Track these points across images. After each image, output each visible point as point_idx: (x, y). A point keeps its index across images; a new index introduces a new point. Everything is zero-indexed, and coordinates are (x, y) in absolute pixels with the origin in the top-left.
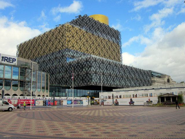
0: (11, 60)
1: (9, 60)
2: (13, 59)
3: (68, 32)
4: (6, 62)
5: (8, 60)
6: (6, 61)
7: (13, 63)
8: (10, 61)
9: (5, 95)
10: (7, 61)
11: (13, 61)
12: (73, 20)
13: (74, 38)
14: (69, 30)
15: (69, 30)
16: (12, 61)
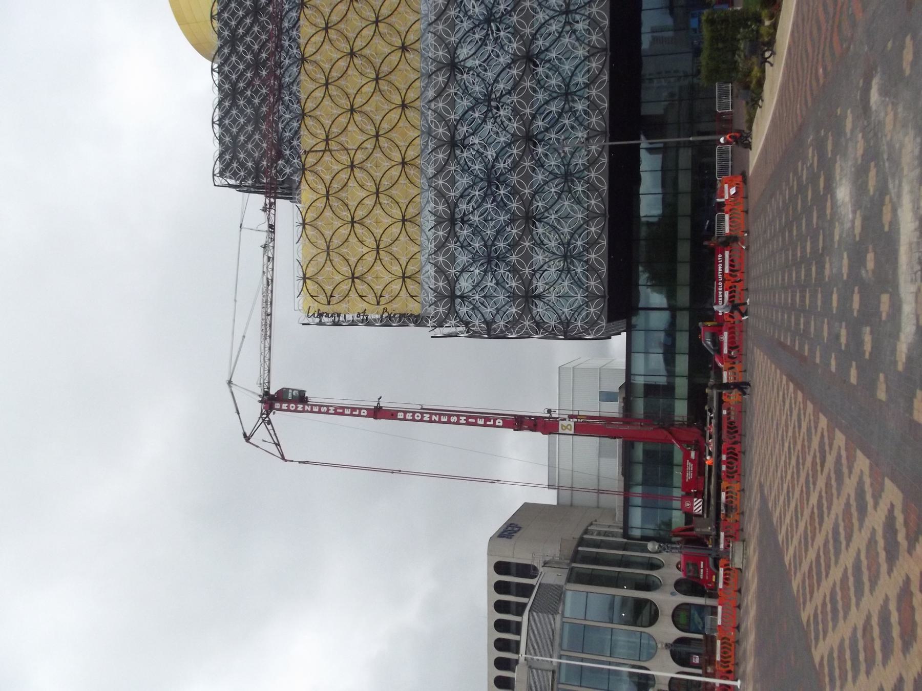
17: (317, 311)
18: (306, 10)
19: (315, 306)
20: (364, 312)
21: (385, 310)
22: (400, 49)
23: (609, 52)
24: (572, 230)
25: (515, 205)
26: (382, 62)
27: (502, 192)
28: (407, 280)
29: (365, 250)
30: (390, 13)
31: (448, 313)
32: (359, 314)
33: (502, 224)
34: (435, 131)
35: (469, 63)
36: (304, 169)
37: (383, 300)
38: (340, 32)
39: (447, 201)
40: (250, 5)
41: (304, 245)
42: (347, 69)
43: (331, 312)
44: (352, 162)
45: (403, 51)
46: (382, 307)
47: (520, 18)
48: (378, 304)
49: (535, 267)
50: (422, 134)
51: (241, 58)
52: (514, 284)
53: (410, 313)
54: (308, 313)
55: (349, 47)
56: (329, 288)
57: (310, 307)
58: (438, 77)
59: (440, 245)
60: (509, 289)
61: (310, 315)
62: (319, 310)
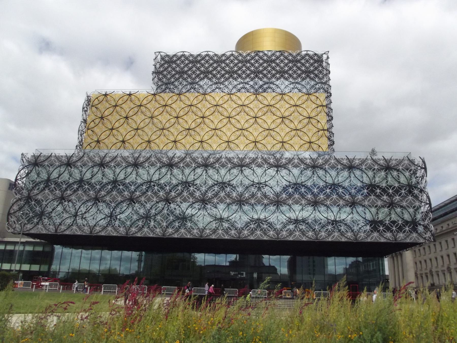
23: (355, 241)
24: (310, 224)
25: (322, 196)
27: (290, 190)
28: (281, 144)
29: (269, 124)
31: (270, 164)
33: (312, 190)
34: (320, 158)
35: (352, 175)
36: (309, 94)
39: (323, 164)
44: (311, 118)
49: (293, 206)
50: (324, 152)
52: (247, 195)
59: (302, 160)
60: (257, 193)
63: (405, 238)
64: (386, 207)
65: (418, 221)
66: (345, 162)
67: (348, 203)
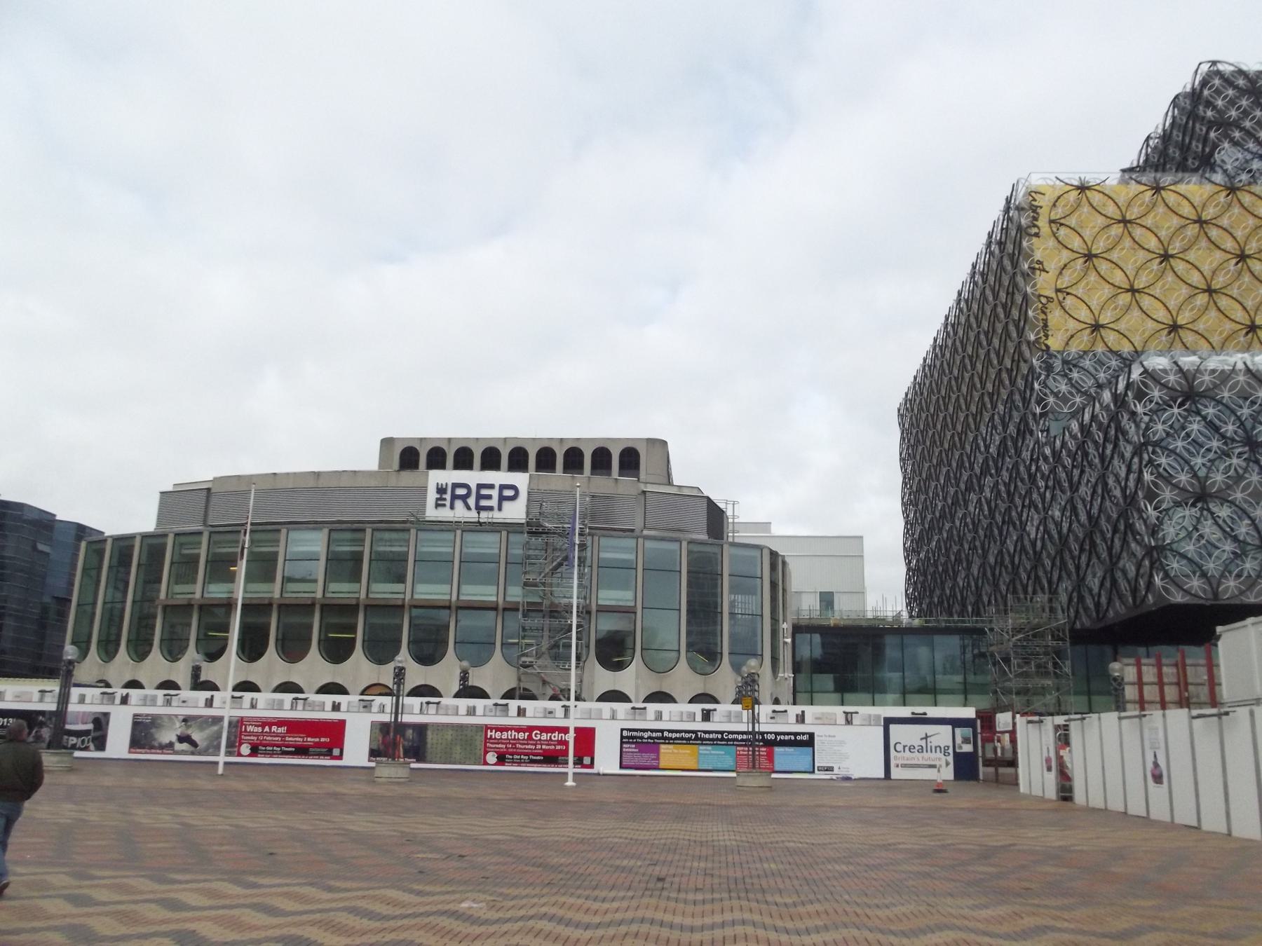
0: (489, 497)
1: (480, 497)
2: (503, 487)
3: (1037, 235)
4: (460, 513)
5: (472, 501)
6: (459, 504)
7: (500, 509)
8: (484, 503)
9: (409, 695)
10: (469, 508)
11: (502, 498)
12: (1148, 138)
13: (1103, 267)
14: (1042, 223)
15: (1052, 222)
16: (494, 502)
17: (1039, 205)
18: (1150, 193)
19: (1044, 202)
20: (1044, 270)
21: (1049, 299)
22: (1095, 320)
26: (1155, 297)
30: (1145, 309)
32: (1041, 263)
37: (1061, 296)
38: (1120, 239)
40: (1231, 116)
41: (1053, 187)
42: (1223, 250)
43: (1039, 223)
45: (1092, 326)
46: (1053, 295)
47: (1255, 485)
48: (1058, 291)
51: (1232, 102)
53: (1050, 333)
54: (1035, 193)
55: (1252, 252)
56: (1072, 221)
57: (1044, 194)
58: (1244, 375)
61: (1033, 194)
62: (1041, 207)
63: (1242, 593)
64: (1186, 504)
65: (1168, 544)
66: (1172, 378)
67: (1188, 495)
